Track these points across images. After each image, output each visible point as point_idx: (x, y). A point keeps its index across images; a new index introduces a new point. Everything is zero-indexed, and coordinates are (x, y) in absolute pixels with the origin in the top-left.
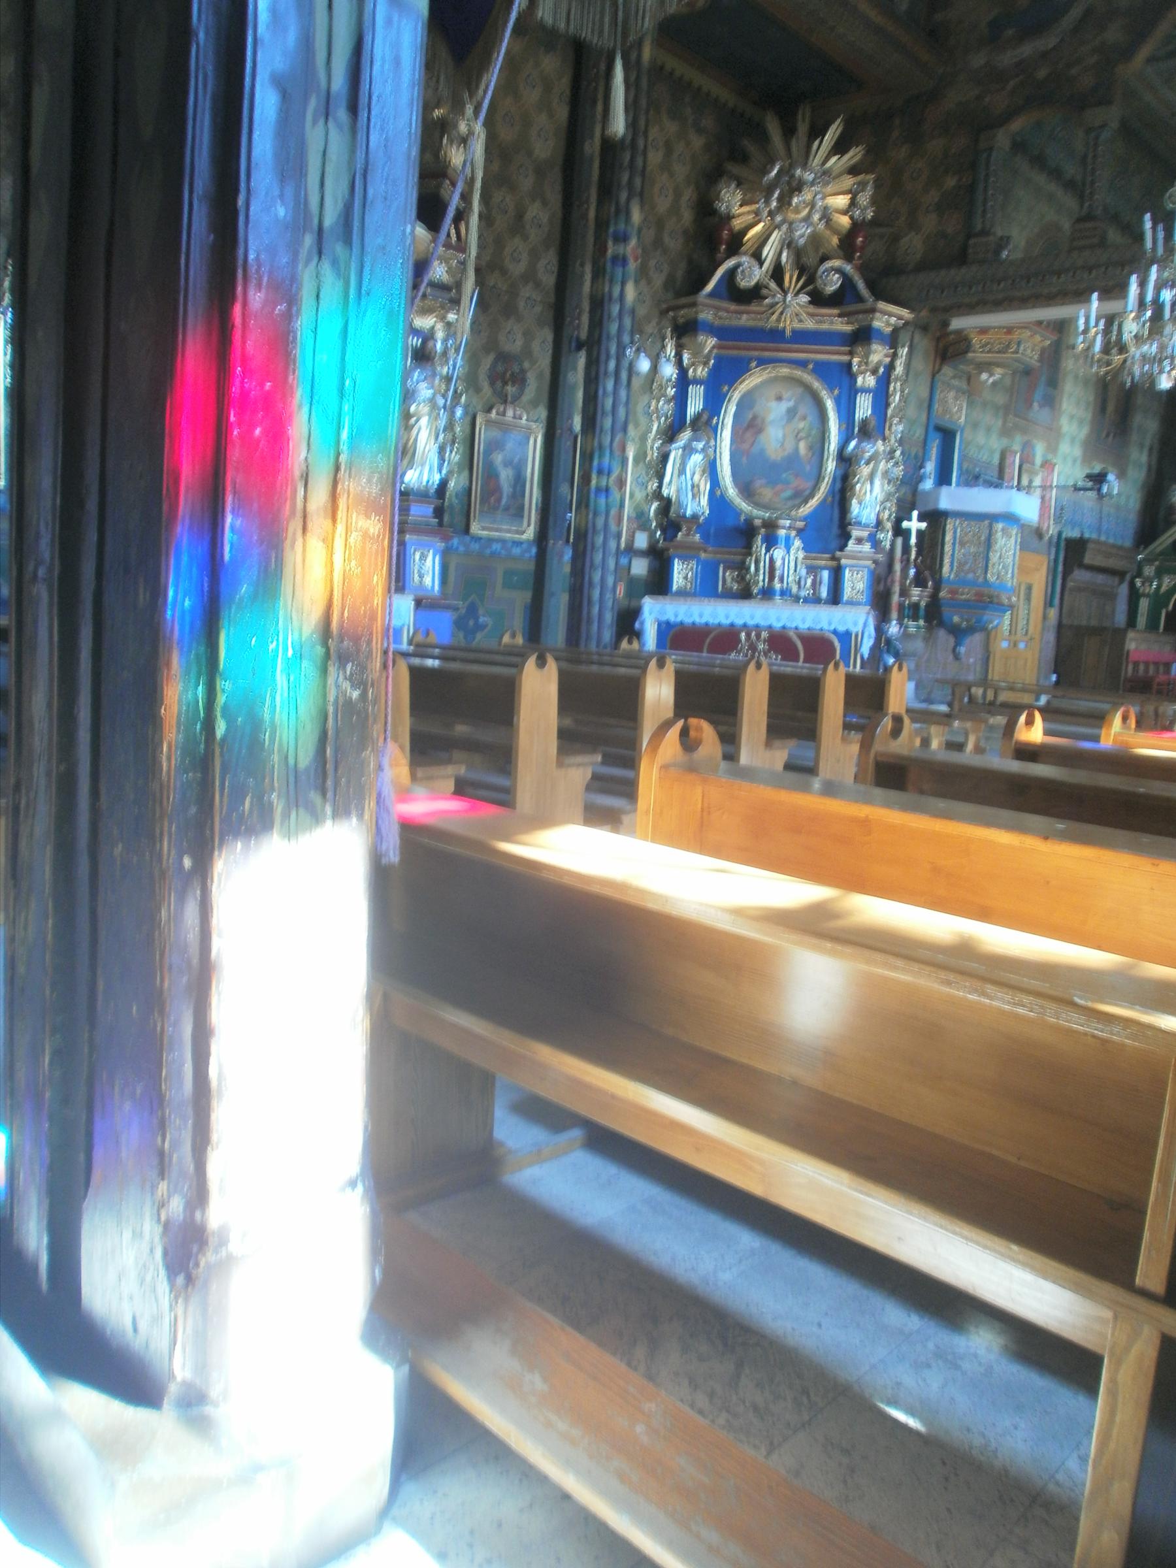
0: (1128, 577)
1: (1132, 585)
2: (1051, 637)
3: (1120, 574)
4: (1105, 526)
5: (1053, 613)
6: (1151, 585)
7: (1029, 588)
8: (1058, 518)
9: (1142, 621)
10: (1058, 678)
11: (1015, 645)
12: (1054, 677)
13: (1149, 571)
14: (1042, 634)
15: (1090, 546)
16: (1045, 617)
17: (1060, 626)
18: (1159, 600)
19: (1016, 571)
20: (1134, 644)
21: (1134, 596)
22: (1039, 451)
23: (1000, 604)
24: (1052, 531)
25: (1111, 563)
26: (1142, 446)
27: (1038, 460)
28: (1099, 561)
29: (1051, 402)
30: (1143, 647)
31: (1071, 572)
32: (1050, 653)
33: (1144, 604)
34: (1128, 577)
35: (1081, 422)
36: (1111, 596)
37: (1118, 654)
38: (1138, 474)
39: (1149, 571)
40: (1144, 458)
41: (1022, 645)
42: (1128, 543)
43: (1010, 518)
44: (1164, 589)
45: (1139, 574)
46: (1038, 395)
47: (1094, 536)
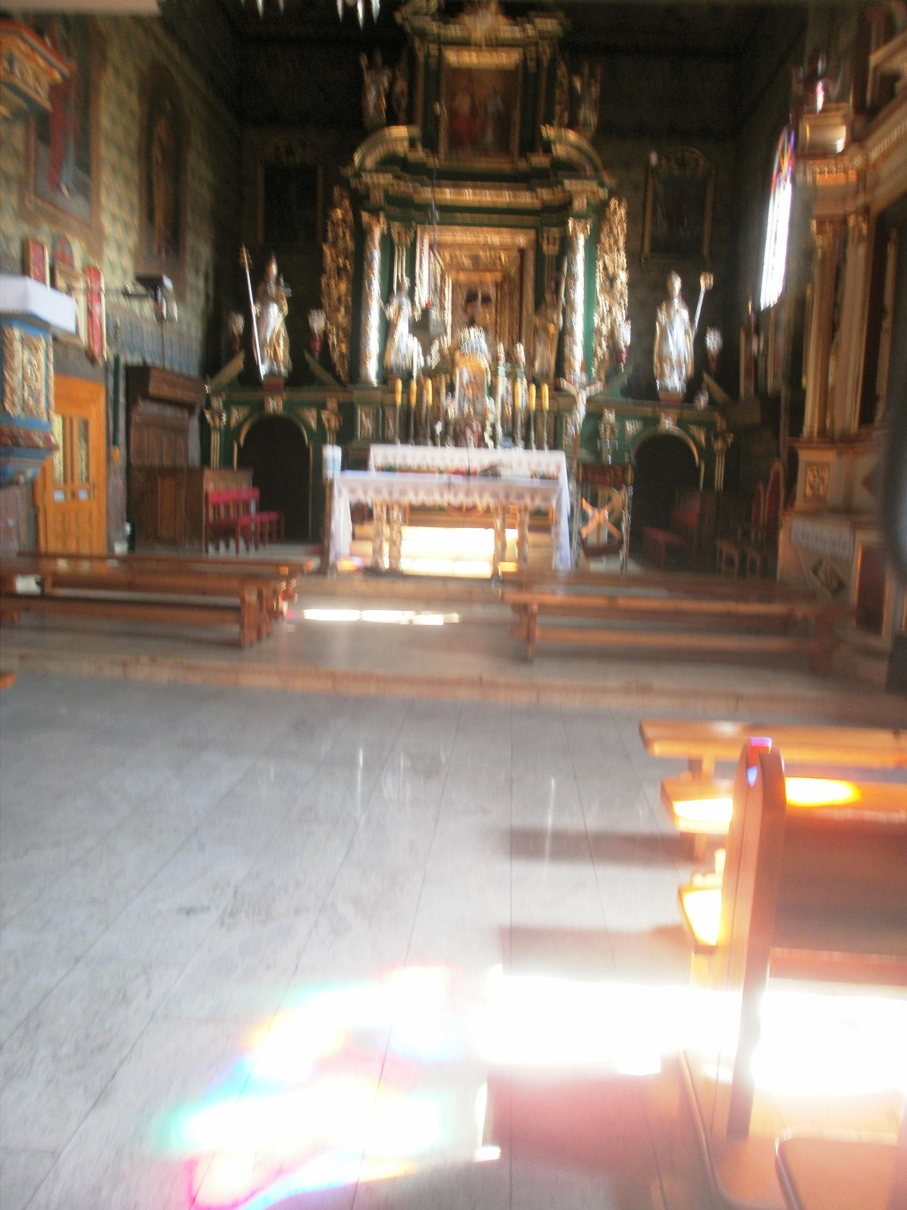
0: (197, 411)
1: (202, 419)
2: (119, 481)
3: (189, 407)
4: (168, 354)
5: (119, 454)
6: (221, 419)
7: (86, 424)
8: (113, 338)
9: (215, 456)
10: (133, 527)
11: (74, 495)
12: (128, 528)
13: (217, 403)
14: (108, 478)
15: (154, 374)
16: (109, 459)
17: (129, 468)
18: (229, 434)
19: (52, 399)
20: (214, 484)
21: (205, 430)
22: (78, 250)
23: (36, 447)
24: (107, 353)
25: (180, 394)
26: (197, 272)
27: (78, 263)
28: (166, 391)
29: (86, 189)
30: (221, 486)
31: (135, 402)
32: (120, 500)
33: (216, 439)
34: (197, 411)
35: (126, 226)
36: (183, 432)
37: (197, 498)
38: (197, 300)
39: (217, 403)
40: (201, 284)
41: (83, 495)
42: (194, 371)
43: (33, 322)
44: (233, 422)
45: (208, 406)
46: (69, 172)
47: (158, 363)
